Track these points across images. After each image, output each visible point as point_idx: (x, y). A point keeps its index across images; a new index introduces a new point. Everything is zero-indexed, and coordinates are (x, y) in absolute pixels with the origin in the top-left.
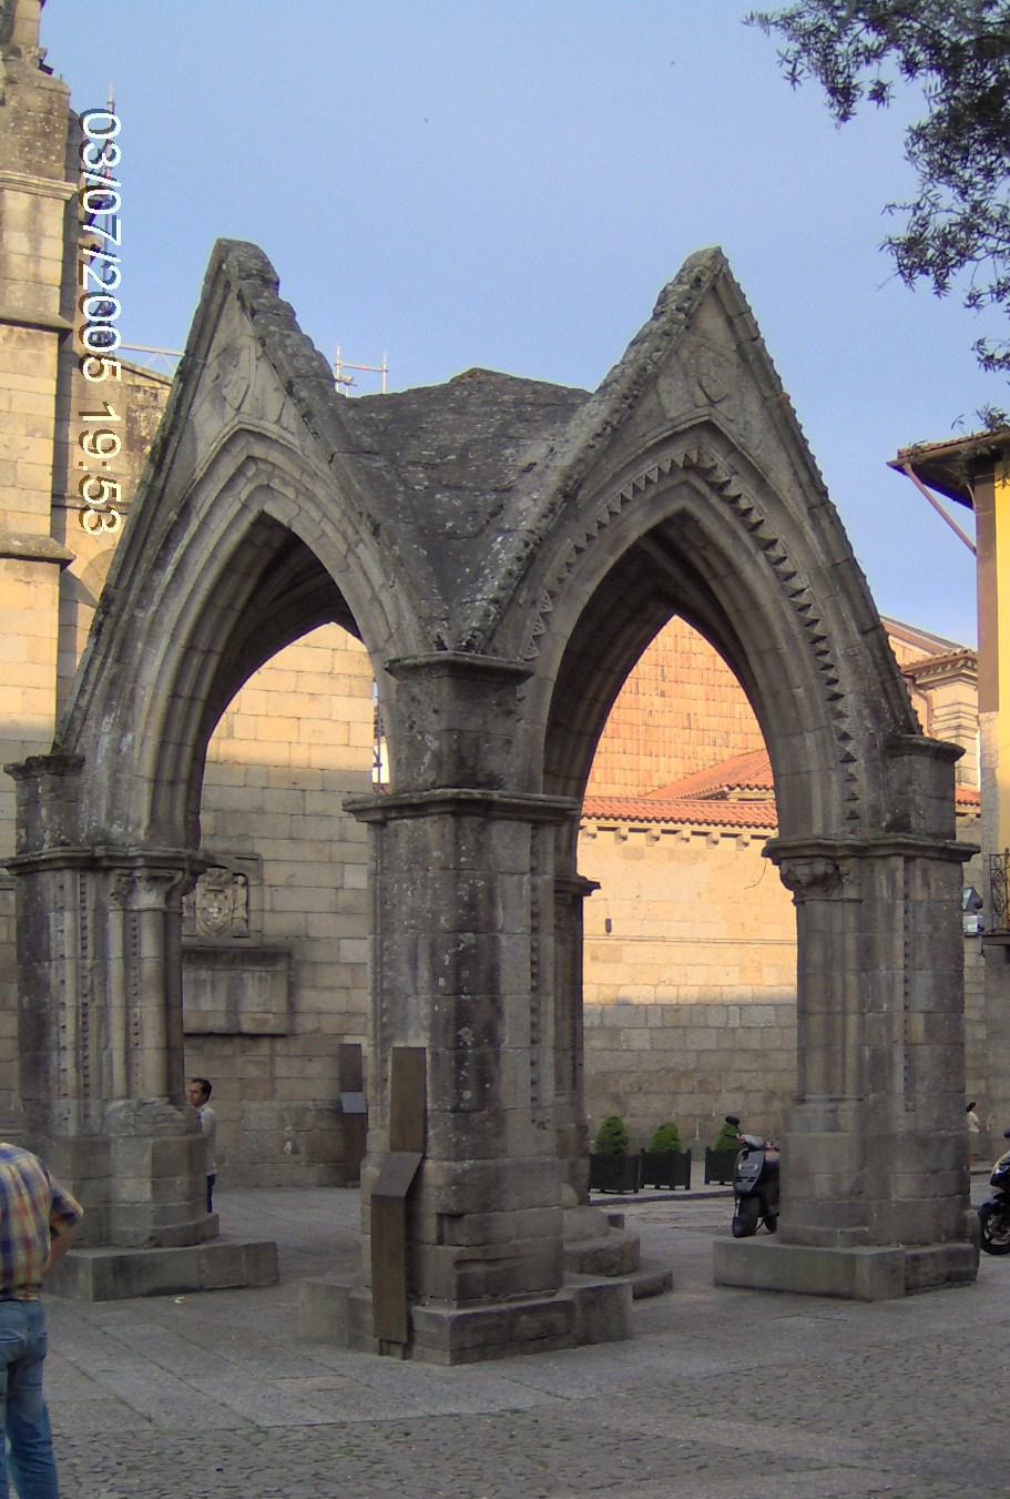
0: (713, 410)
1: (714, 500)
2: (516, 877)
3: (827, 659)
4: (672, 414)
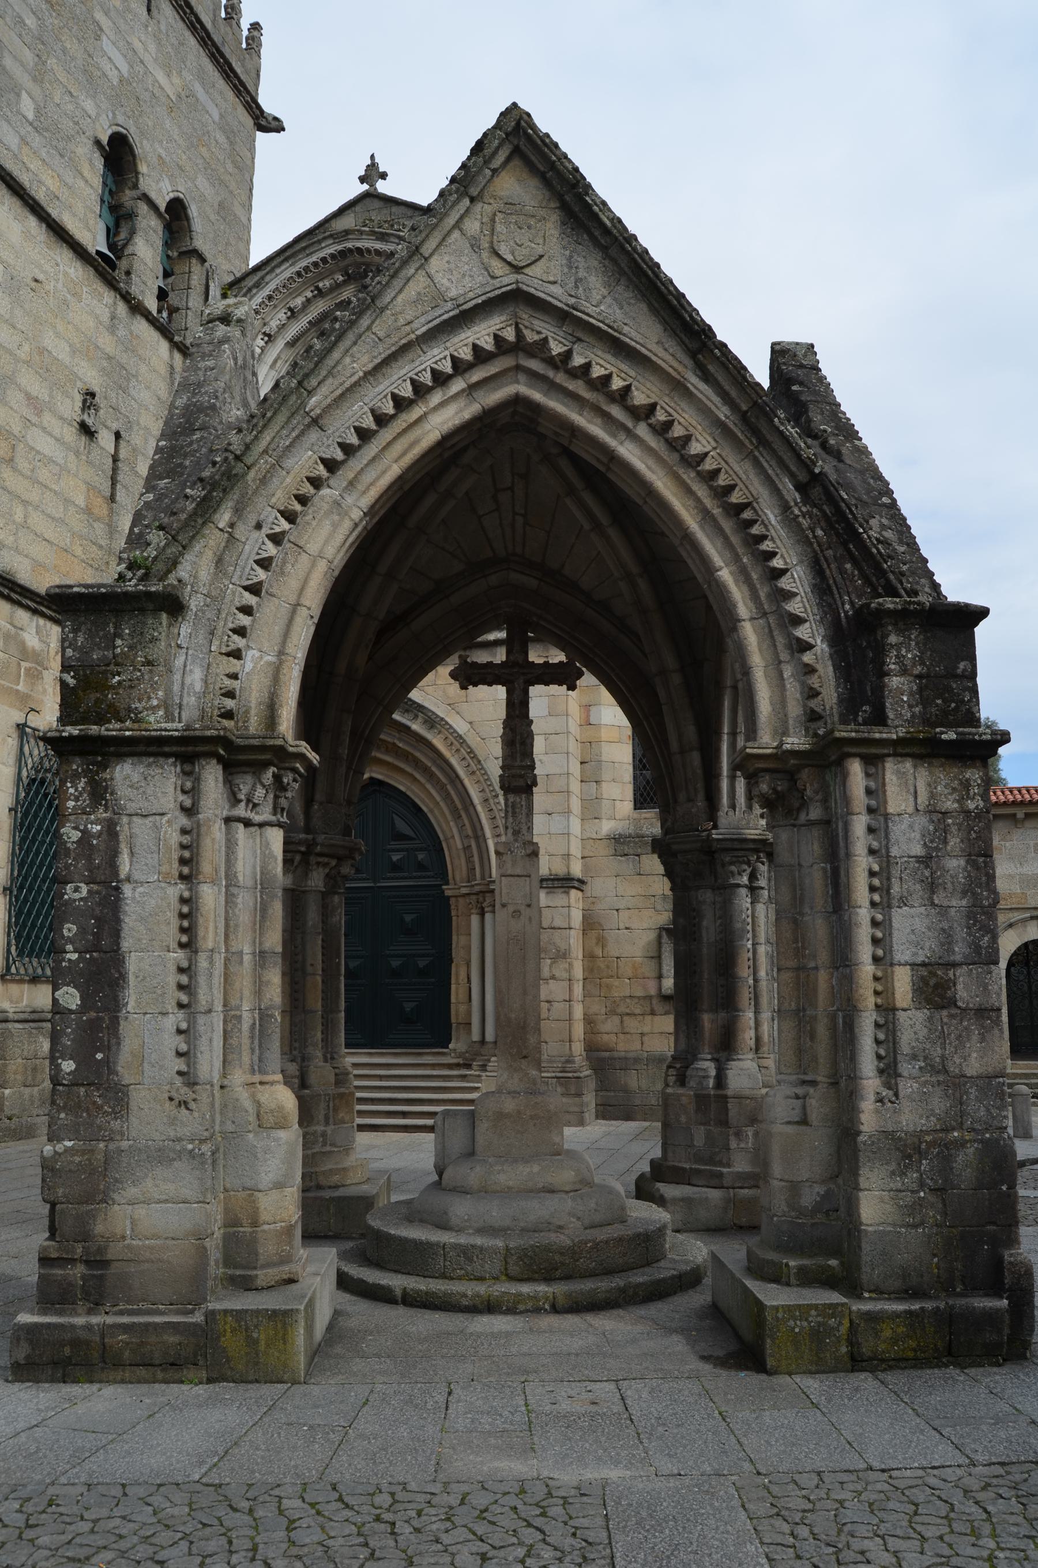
0: (519, 277)
1: (560, 378)
2: (151, 819)
3: (756, 530)
4: (453, 293)
